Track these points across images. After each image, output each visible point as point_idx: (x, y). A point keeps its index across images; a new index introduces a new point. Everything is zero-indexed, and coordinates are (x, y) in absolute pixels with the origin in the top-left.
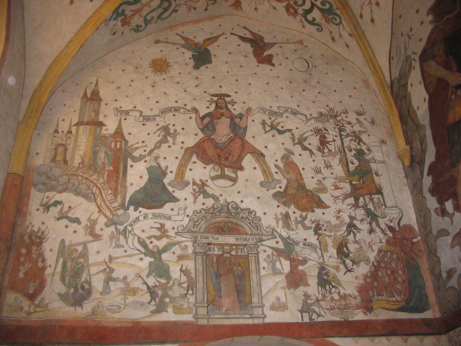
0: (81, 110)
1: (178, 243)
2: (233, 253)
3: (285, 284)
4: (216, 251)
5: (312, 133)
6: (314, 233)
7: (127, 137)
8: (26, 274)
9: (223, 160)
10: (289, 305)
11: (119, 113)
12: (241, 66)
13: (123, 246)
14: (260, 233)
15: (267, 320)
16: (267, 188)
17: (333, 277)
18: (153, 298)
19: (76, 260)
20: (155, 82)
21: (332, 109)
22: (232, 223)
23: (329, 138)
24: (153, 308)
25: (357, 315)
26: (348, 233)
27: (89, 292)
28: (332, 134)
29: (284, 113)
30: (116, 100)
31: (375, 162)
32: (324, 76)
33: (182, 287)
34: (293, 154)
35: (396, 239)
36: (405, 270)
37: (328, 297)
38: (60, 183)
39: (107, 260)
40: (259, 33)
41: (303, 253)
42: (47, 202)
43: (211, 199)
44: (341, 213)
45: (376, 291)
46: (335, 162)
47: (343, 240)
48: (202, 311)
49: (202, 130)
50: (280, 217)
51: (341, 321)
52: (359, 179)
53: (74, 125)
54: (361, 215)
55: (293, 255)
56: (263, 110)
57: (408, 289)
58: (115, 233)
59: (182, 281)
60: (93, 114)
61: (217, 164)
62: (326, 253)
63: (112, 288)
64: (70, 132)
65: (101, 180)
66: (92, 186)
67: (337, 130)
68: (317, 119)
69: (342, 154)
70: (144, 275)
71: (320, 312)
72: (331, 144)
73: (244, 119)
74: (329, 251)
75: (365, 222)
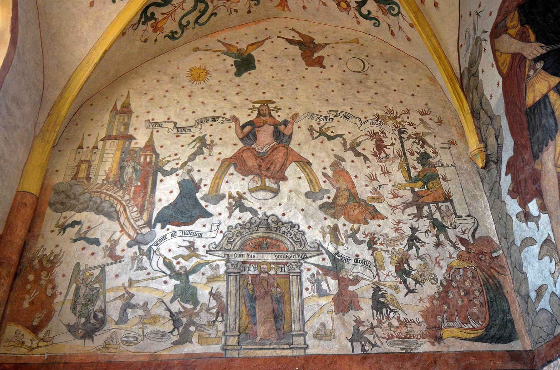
0: (109, 124)
1: (208, 263)
2: (272, 272)
3: (333, 308)
4: (252, 271)
5: (367, 137)
6: (368, 248)
7: (158, 150)
8: (32, 303)
9: (264, 171)
10: (337, 334)
11: (151, 126)
12: (288, 70)
13: (145, 268)
15: (309, 352)
17: (391, 299)
18: (176, 327)
19: (90, 285)
20: (192, 92)
22: (270, 238)
23: (387, 142)
24: (175, 338)
25: (422, 345)
26: (409, 247)
27: (103, 322)
28: (390, 137)
30: (148, 112)
31: (443, 165)
32: (382, 75)
33: (211, 313)
34: (344, 160)
37: (384, 323)
38: (80, 202)
39: (126, 284)
40: (309, 35)
41: (355, 270)
42: (64, 223)
43: (248, 213)
44: (401, 225)
45: (447, 317)
46: (394, 167)
48: (233, 341)
49: (242, 139)
53: (101, 140)
54: (426, 227)
55: (343, 274)
56: (311, 115)
57: (487, 314)
58: (138, 254)
59: (211, 306)
60: (122, 128)
61: (257, 175)
62: (383, 271)
63: (130, 316)
64: (96, 147)
65: (127, 197)
66: (116, 203)
67: (396, 132)
68: (373, 122)
69: (403, 158)
70: (167, 300)
71: (375, 342)
73: (289, 126)
75: (430, 234)
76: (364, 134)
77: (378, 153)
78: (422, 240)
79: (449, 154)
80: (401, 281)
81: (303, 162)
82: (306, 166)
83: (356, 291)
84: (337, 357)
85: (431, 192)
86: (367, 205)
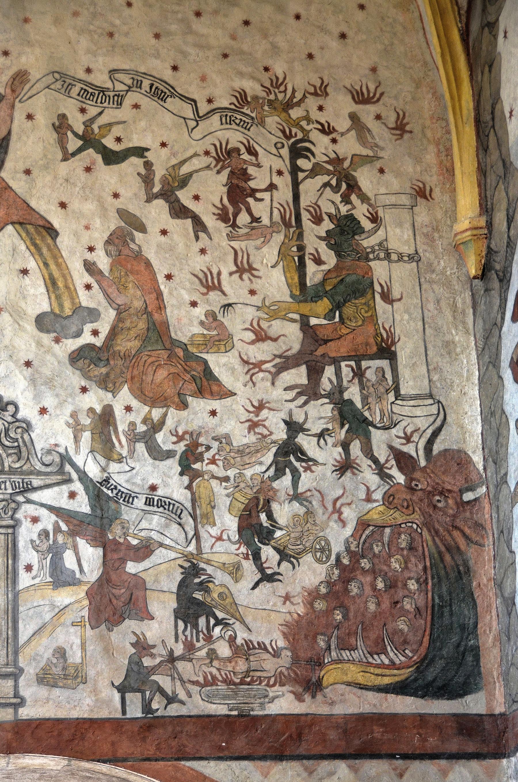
3: (85, 613)
5: (209, 160)
6: (179, 469)
10: (91, 673)
14: (25, 468)
15: (25, 713)
16: (55, 334)
17: (220, 595)
21: (280, 81)
25: (276, 701)
26: (276, 470)
29: (127, 91)
31: (388, 256)
34: (143, 229)
35: (416, 490)
36: (426, 581)
37: (200, 649)
41: (144, 524)
44: (264, 413)
45: (338, 638)
47: (258, 492)
50: (86, 421)
51: (228, 716)
52: (331, 310)
54: (322, 421)
67: (285, 152)
71: (174, 692)
72: (262, 200)
74: (218, 522)
76: (202, 153)
77: (231, 210)
78: (311, 453)
79: (408, 225)
80: (247, 554)
81: (37, 226)
82: (43, 239)
83: (142, 575)
84: (86, 726)
85: (348, 331)
86: (189, 356)
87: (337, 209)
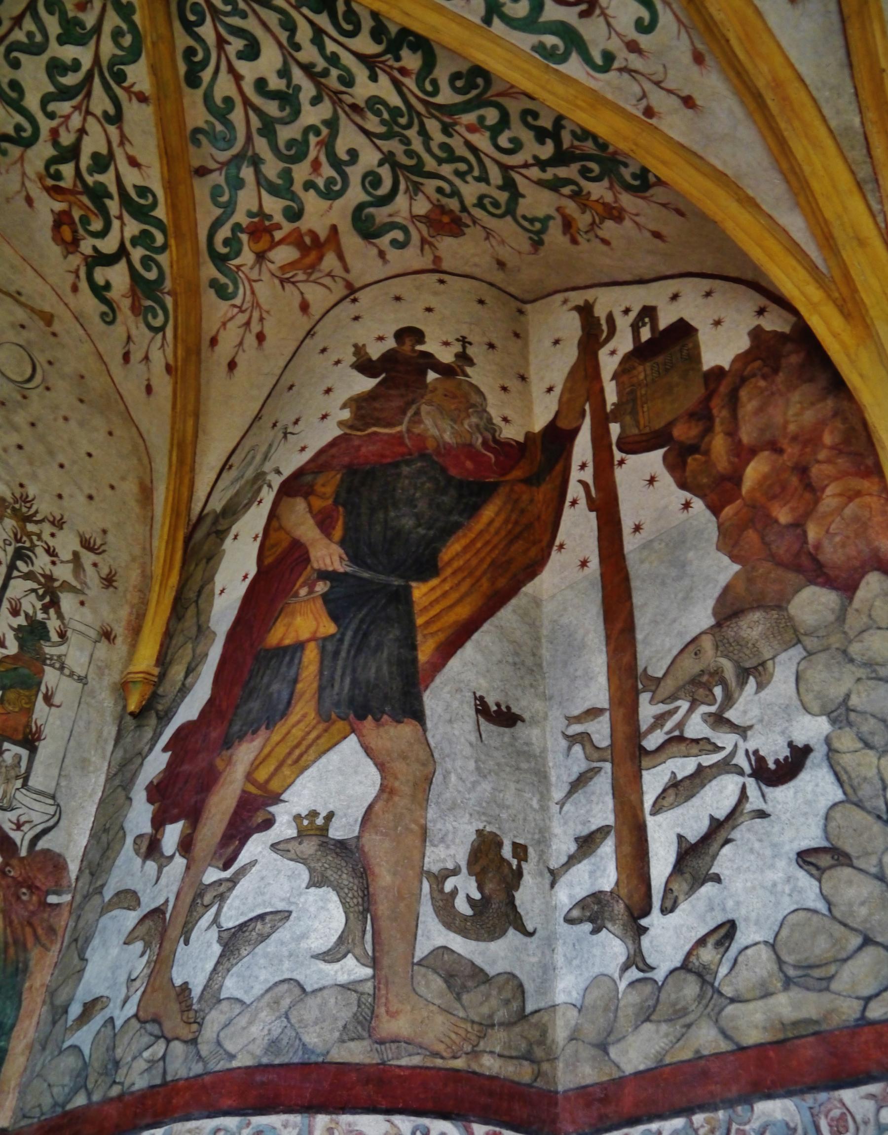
31: (62, 668)
67: (10, 550)
79: (87, 654)
87: (35, 612)
